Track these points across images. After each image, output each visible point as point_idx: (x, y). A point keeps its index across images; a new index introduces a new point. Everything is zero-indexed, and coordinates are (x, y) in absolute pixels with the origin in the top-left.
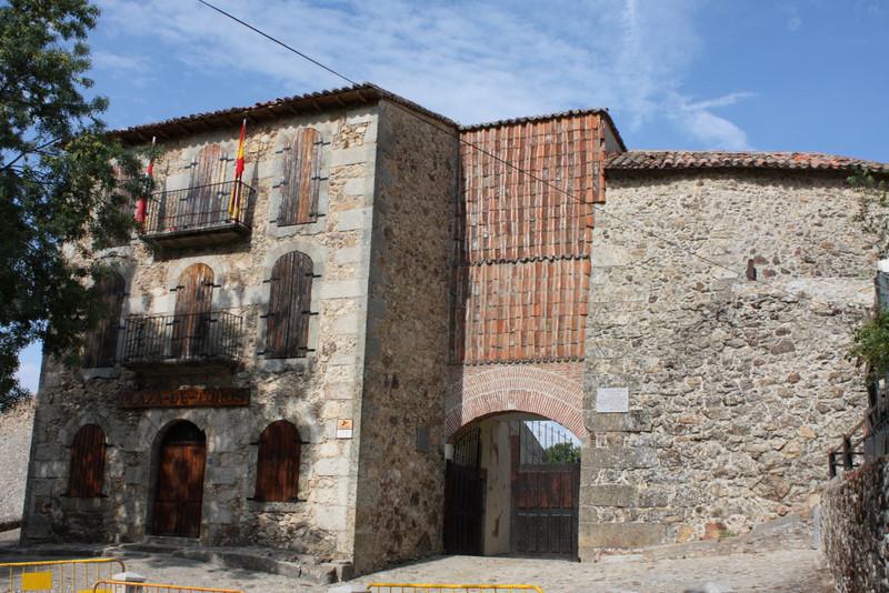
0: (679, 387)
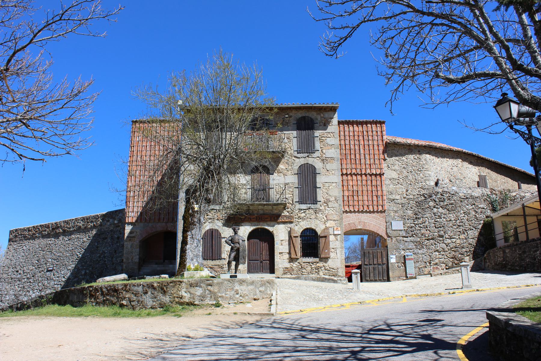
0: (420, 221)
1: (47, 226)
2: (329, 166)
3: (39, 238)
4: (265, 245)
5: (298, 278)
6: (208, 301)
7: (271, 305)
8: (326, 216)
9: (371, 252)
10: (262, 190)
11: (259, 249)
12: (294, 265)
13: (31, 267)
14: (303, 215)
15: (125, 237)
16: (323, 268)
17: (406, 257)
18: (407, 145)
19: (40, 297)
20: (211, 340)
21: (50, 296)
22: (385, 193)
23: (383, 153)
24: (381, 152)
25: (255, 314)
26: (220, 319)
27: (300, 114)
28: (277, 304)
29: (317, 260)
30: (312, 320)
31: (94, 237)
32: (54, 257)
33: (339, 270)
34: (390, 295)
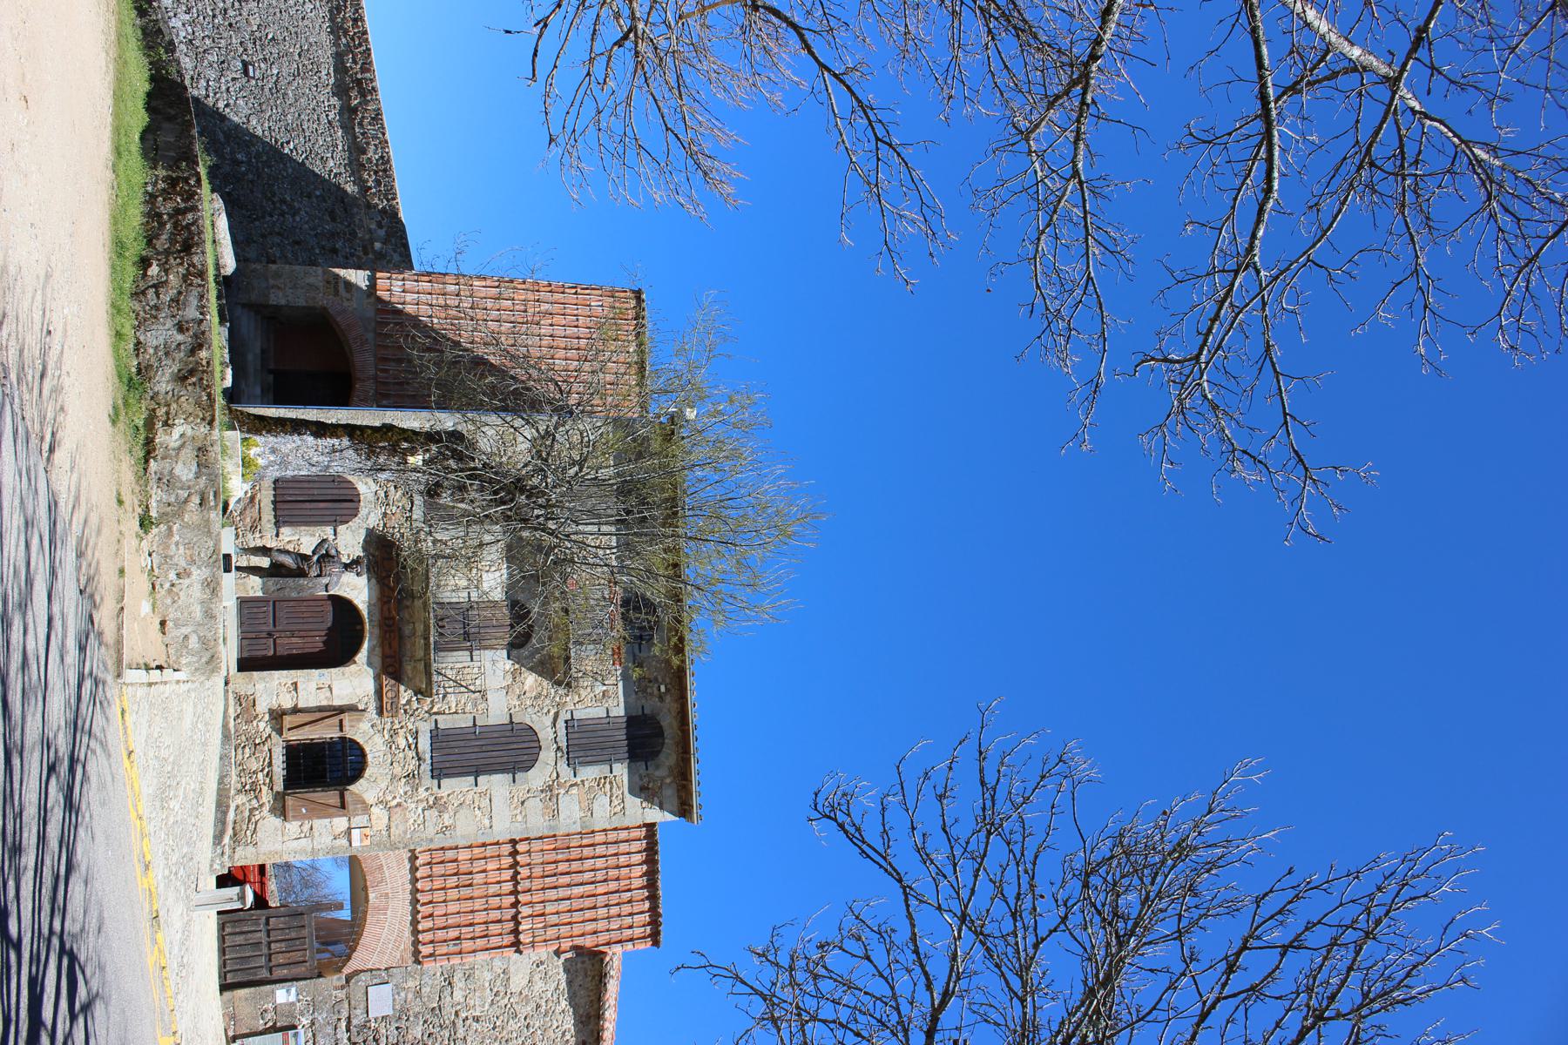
1: (367, 67)
2: (535, 805)
3: (336, 44)
4: (316, 643)
5: (226, 737)
6: (157, 496)
7: (148, 668)
8: (399, 805)
9: (305, 932)
10: (466, 630)
11: (305, 627)
12: (262, 725)
13: (255, 22)
14: (402, 743)
15: (336, 270)
16: (255, 803)
18: (599, 1008)
19: (171, 43)
20: (43, 512)
21: (173, 70)
22: (470, 959)
23: (575, 948)
24: (579, 941)
25: (120, 628)
26: (105, 531)
27: (668, 722)
28: (150, 685)
29: (279, 786)
30: (102, 786)
31: (338, 187)
32: (283, 82)
33: (250, 848)
34: (180, 997)
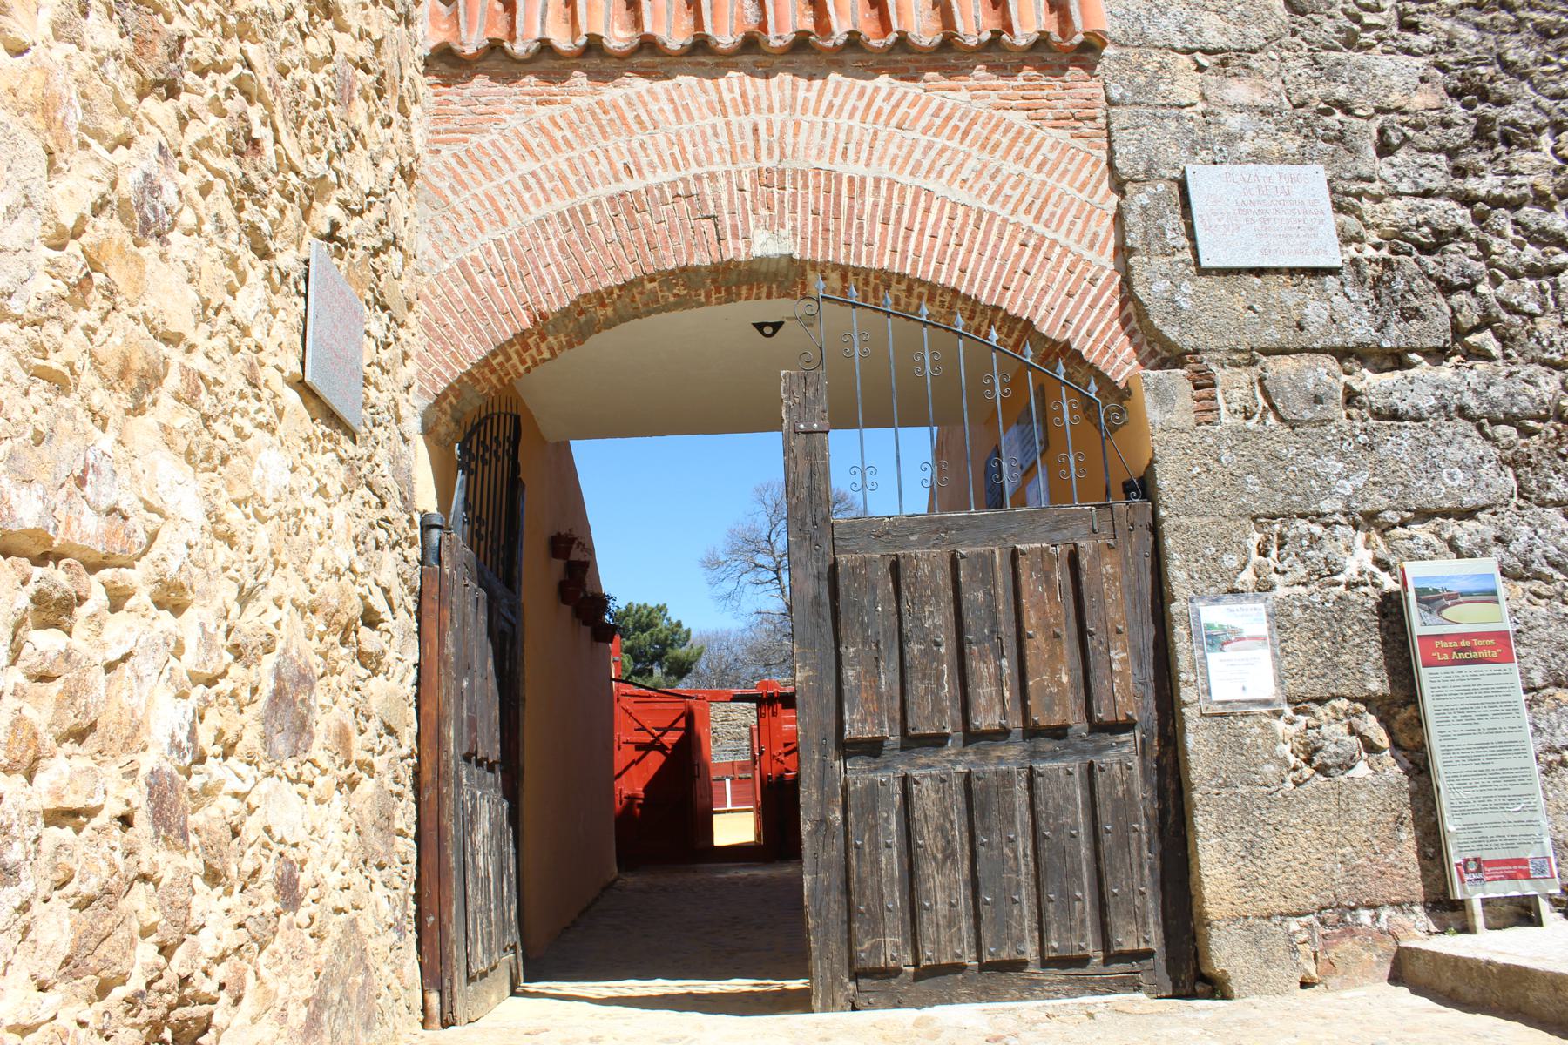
9: (927, 562)
17: (1420, 624)
